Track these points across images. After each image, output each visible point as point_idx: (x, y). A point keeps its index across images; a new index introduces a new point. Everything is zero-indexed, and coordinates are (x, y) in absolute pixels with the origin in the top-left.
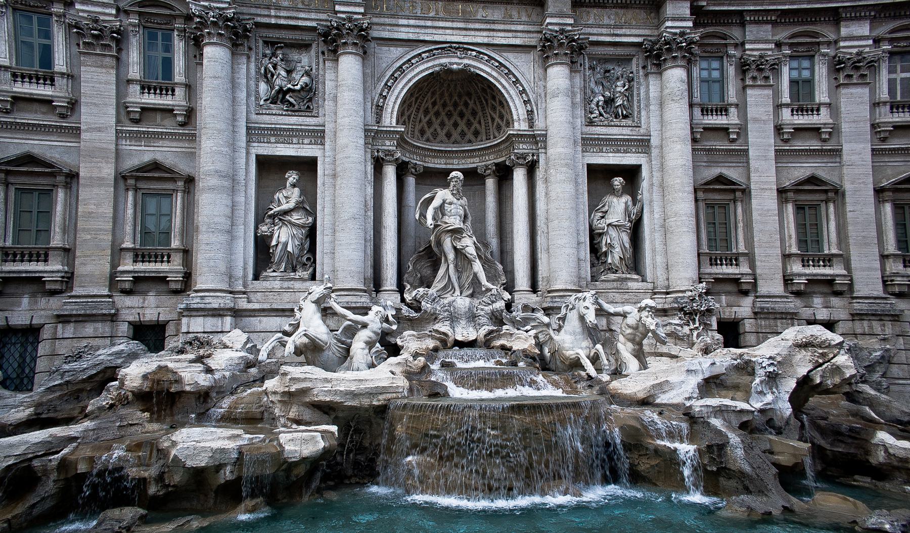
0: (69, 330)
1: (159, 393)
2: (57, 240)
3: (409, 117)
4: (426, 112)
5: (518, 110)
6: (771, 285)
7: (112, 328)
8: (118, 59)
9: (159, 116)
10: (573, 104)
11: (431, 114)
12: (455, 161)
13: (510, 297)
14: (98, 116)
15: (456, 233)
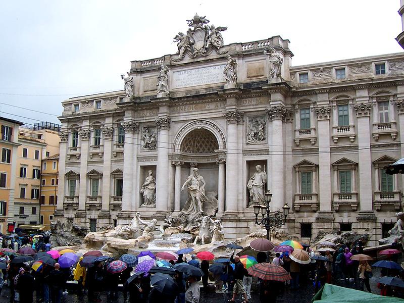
0: (100, 221)
1: (90, 241)
2: (99, 194)
3: (191, 146)
4: (199, 142)
5: (220, 143)
6: (325, 207)
7: (110, 221)
8: (112, 138)
9: (120, 154)
10: (238, 138)
11: (201, 142)
12: (210, 160)
13: (214, 213)
14: (107, 157)
15: (194, 190)
